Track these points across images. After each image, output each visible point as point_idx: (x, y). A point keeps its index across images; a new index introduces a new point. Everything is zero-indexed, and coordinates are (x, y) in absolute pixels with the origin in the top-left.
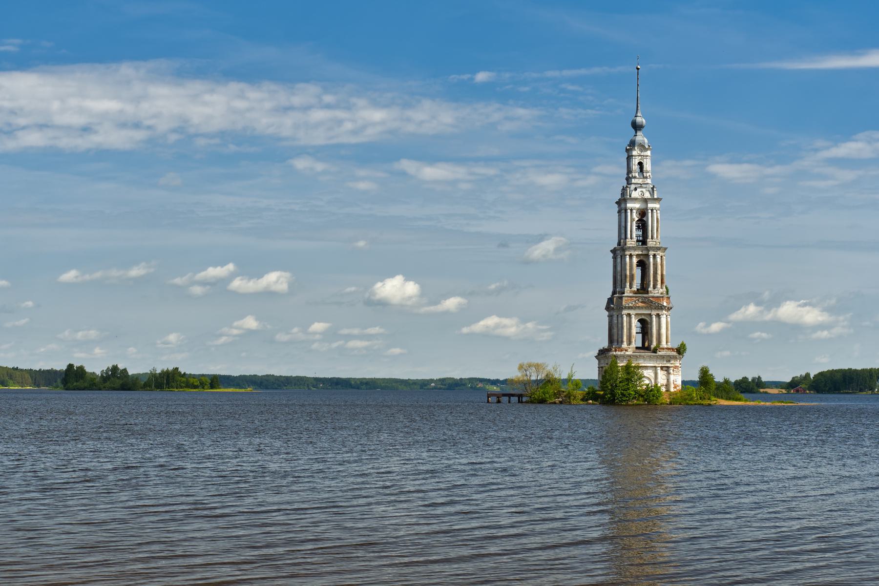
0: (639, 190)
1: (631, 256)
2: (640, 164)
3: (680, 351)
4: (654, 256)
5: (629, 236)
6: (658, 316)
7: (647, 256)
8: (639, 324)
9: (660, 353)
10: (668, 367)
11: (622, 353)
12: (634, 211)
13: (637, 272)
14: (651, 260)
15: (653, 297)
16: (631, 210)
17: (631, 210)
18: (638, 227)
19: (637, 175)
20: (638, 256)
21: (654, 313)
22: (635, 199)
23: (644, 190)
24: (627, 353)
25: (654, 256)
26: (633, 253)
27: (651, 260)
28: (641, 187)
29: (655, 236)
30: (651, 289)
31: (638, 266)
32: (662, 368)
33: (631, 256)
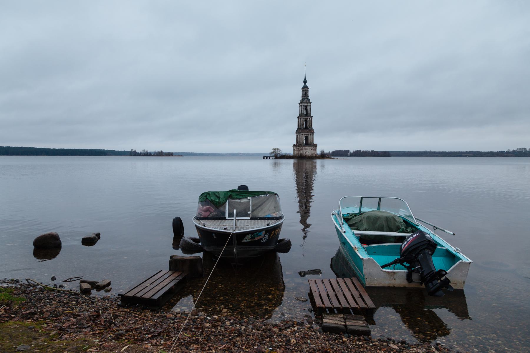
22: (305, 103)
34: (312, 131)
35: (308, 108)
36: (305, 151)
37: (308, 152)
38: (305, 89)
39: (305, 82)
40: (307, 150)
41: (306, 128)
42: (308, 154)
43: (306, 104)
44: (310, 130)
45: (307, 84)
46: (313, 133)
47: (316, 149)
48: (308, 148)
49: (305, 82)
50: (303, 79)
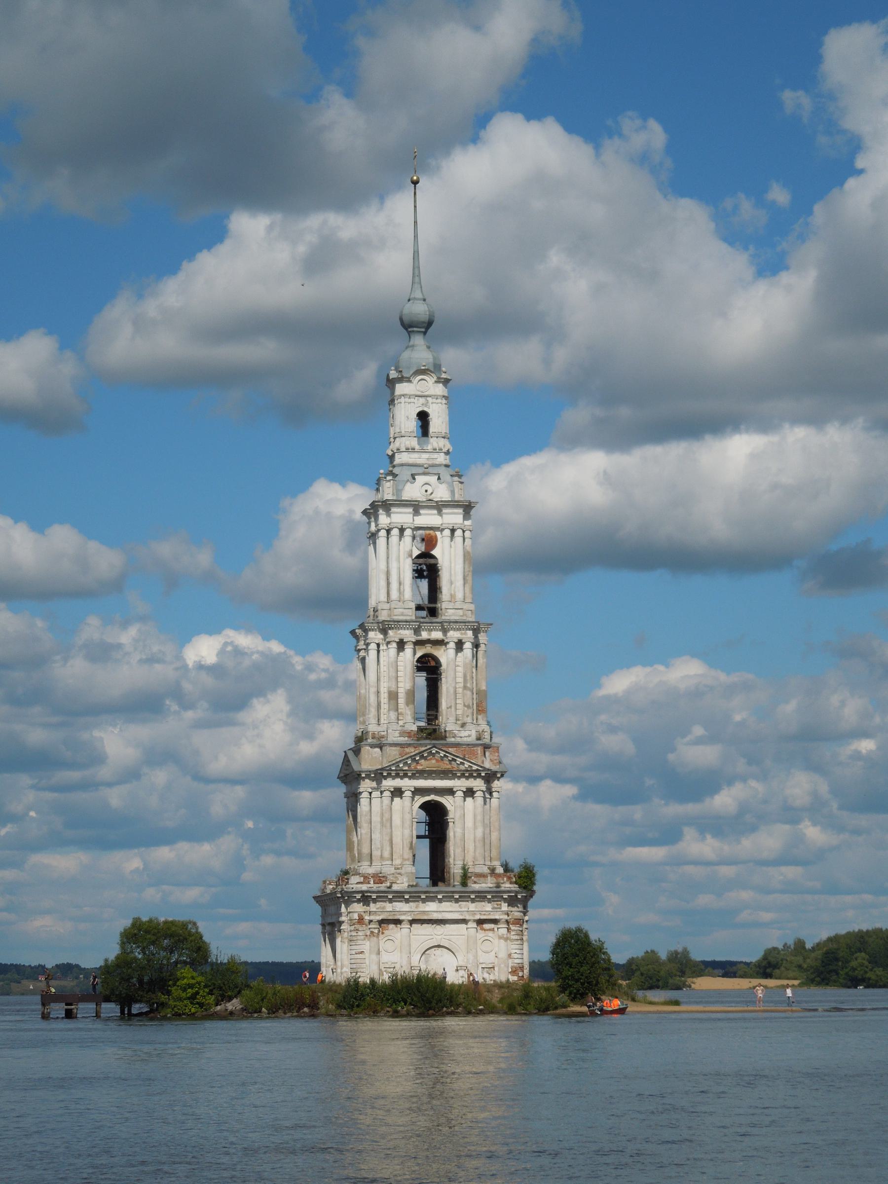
0: (420, 479)
1: (401, 645)
2: (423, 417)
3: (526, 879)
4: (459, 645)
5: (394, 595)
6: (470, 793)
9: (477, 887)
10: (495, 921)
11: (383, 887)
12: (408, 532)
15: (457, 745)
16: (402, 530)
17: (402, 530)
18: (419, 574)
19: (414, 443)
24: (395, 887)
25: (459, 645)
26: (407, 634)
28: (424, 474)
31: (419, 669)
32: (480, 922)
33: (401, 645)
36: (425, 934)
43: (428, 518)
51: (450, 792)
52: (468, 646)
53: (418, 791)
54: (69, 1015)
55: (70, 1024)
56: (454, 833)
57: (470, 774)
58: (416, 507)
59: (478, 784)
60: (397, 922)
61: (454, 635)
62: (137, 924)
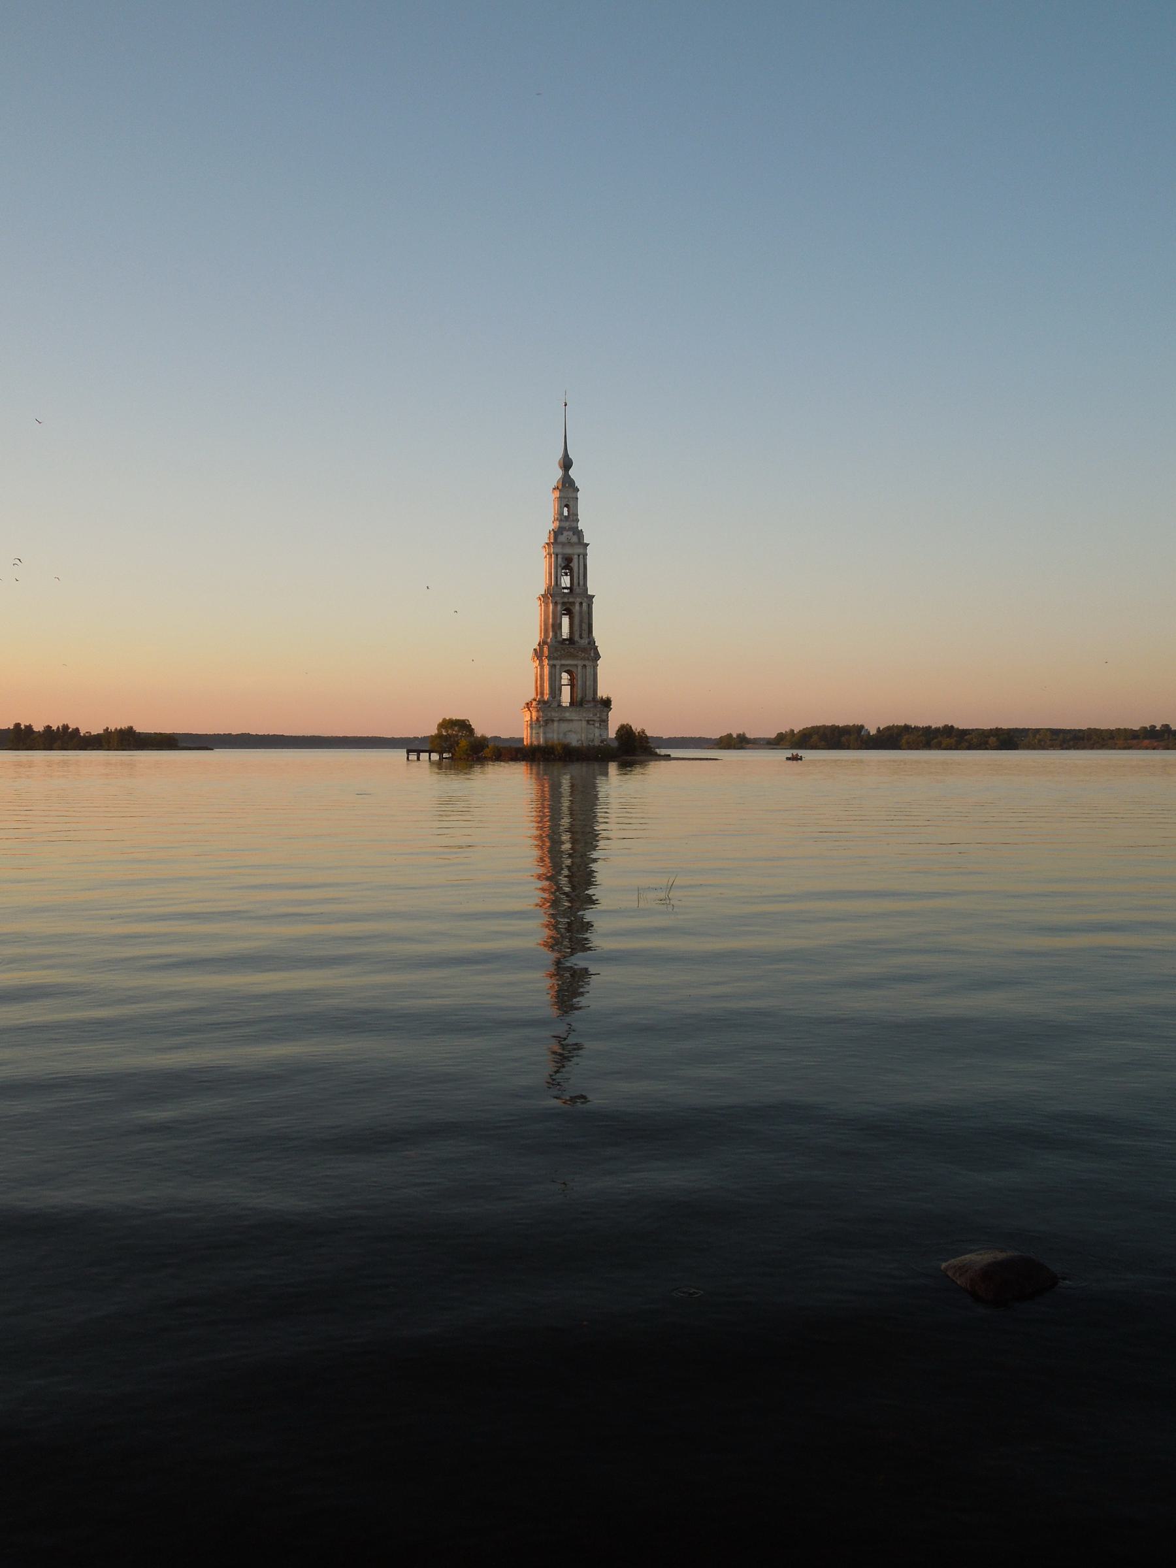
0: (565, 533)
1: (556, 604)
7: (573, 603)
8: (565, 676)
13: (565, 621)
14: (577, 607)
20: (564, 604)
21: (580, 663)
22: (563, 544)
23: (571, 533)
25: (581, 604)
27: (577, 607)
29: (582, 583)
30: (577, 638)
34: (591, 654)
35: (574, 565)
36: (565, 726)
37: (576, 733)
38: (567, 489)
39: (567, 464)
40: (575, 726)
41: (571, 640)
42: (574, 740)
43: (568, 551)
44: (584, 650)
45: (571, 472)
46: (597, 656)
47: (604, 722)
48: (574, 716)
49: (567, 464)
50: (561, 454)
51: (576, 666)
52: (584, 605)
53: (562, 665)
54: (418, 759)
55: (417, 763)
56: (579, 683)
57: (583, 659)
58: (563, 544)
59: (587, 663)
60: (553, 721)
61: (579, 600)
62: (444, 720)
